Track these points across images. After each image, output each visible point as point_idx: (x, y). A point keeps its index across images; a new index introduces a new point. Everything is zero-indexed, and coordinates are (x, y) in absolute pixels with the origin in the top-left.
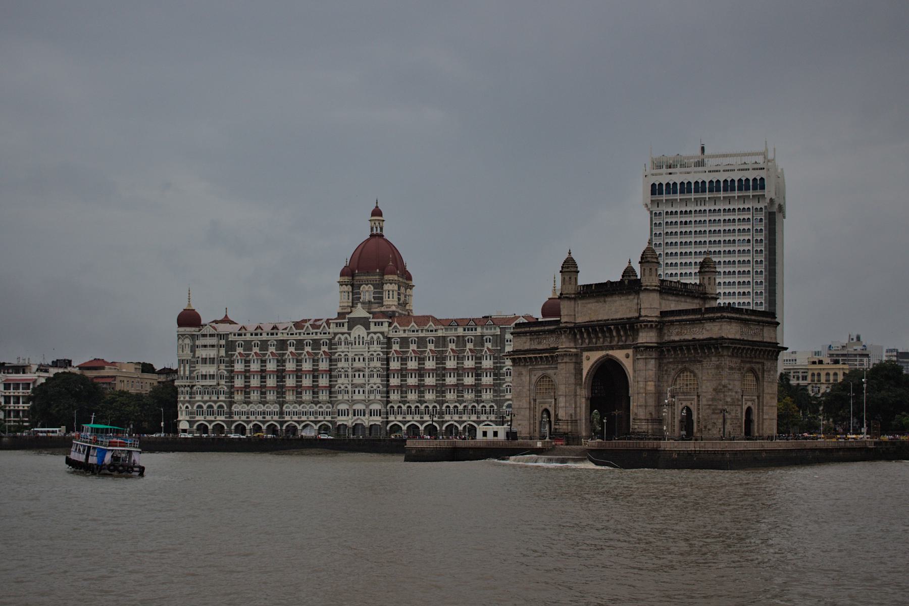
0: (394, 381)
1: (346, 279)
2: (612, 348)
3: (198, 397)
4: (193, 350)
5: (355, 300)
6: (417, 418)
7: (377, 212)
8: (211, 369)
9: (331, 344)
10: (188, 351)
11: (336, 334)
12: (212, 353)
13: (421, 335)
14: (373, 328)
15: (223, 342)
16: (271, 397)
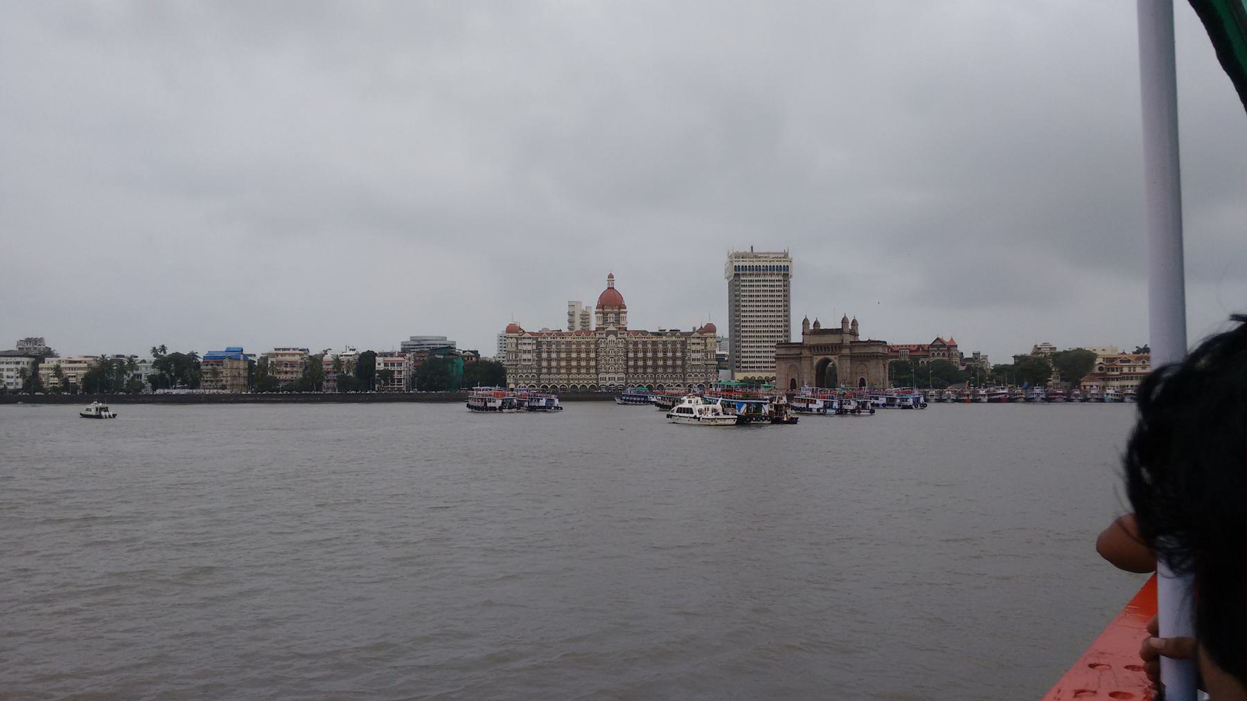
0: (631, 363)
1: (601, 310)
2: (828, 355)
3: (520, 371)
4: (517, 345)
5: (605, 320)
6: (662, 381)
7: (611, 276)
8: (529, 356)
9: (596, 344)
10: (514, 345)
11: (599, 339)
12: (529, 348)
13: (644, 340)
14: (619, 336)
15: (535, 342)
16: (563, 371)
